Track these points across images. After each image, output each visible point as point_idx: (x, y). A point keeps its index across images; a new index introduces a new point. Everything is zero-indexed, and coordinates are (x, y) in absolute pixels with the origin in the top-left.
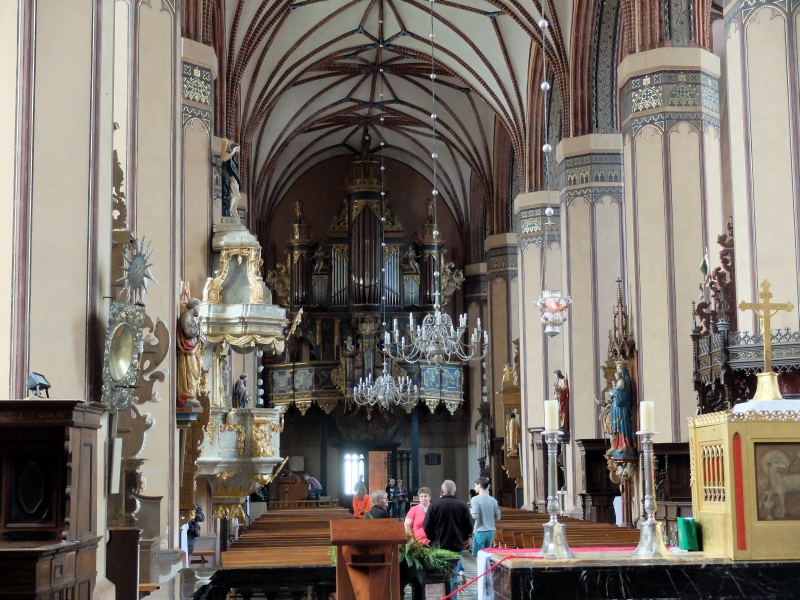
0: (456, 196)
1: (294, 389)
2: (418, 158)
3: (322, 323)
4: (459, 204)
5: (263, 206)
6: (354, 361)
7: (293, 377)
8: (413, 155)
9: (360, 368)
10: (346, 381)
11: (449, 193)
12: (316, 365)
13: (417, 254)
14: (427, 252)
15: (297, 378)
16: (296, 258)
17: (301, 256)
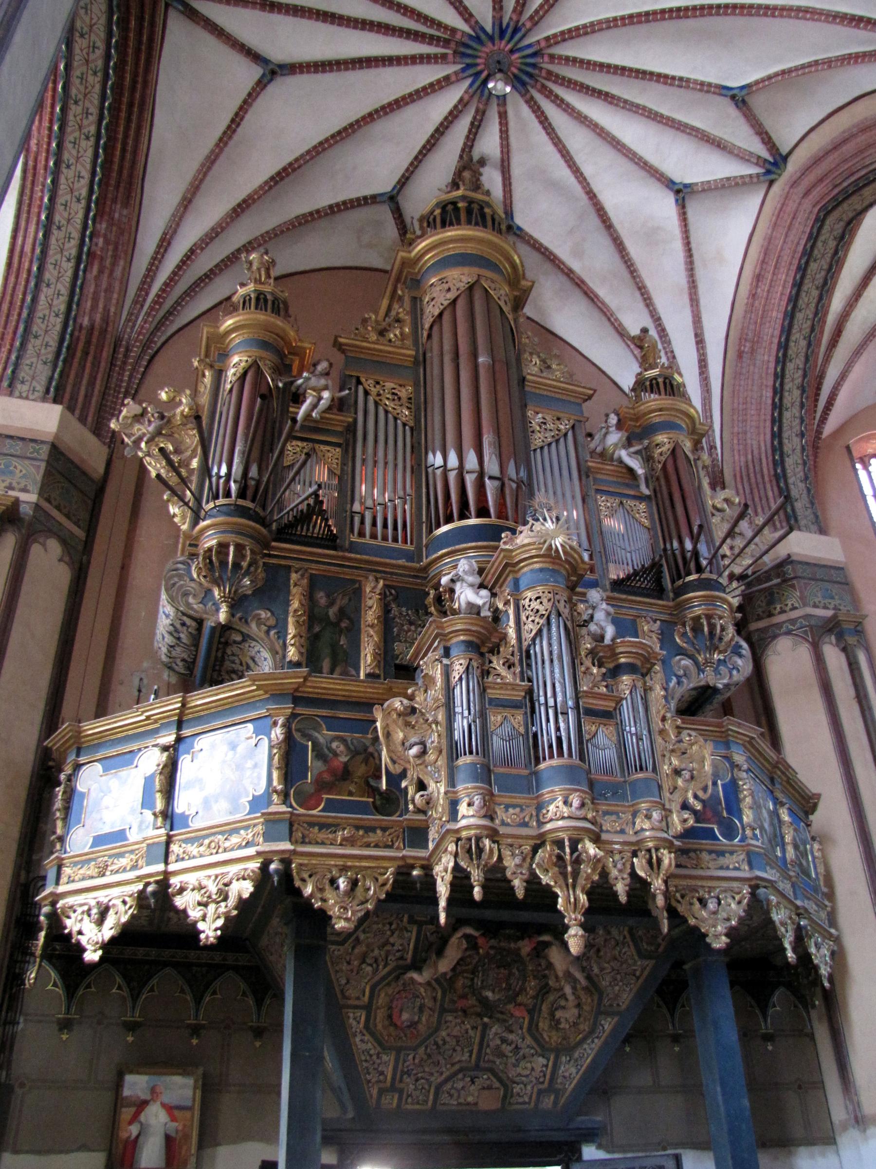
1: (168, 816)
2: (580, 284)
3: (314, 584)
5: (139, 302)
6: (485, 673)
7: (170, 771)
8: (569, 273)
9: (515, 705)
10: (453, 752)
12: (298, 699)
14: (661, 438)
15: (186, 768)
16: (231, 374)
17: (254, 367)
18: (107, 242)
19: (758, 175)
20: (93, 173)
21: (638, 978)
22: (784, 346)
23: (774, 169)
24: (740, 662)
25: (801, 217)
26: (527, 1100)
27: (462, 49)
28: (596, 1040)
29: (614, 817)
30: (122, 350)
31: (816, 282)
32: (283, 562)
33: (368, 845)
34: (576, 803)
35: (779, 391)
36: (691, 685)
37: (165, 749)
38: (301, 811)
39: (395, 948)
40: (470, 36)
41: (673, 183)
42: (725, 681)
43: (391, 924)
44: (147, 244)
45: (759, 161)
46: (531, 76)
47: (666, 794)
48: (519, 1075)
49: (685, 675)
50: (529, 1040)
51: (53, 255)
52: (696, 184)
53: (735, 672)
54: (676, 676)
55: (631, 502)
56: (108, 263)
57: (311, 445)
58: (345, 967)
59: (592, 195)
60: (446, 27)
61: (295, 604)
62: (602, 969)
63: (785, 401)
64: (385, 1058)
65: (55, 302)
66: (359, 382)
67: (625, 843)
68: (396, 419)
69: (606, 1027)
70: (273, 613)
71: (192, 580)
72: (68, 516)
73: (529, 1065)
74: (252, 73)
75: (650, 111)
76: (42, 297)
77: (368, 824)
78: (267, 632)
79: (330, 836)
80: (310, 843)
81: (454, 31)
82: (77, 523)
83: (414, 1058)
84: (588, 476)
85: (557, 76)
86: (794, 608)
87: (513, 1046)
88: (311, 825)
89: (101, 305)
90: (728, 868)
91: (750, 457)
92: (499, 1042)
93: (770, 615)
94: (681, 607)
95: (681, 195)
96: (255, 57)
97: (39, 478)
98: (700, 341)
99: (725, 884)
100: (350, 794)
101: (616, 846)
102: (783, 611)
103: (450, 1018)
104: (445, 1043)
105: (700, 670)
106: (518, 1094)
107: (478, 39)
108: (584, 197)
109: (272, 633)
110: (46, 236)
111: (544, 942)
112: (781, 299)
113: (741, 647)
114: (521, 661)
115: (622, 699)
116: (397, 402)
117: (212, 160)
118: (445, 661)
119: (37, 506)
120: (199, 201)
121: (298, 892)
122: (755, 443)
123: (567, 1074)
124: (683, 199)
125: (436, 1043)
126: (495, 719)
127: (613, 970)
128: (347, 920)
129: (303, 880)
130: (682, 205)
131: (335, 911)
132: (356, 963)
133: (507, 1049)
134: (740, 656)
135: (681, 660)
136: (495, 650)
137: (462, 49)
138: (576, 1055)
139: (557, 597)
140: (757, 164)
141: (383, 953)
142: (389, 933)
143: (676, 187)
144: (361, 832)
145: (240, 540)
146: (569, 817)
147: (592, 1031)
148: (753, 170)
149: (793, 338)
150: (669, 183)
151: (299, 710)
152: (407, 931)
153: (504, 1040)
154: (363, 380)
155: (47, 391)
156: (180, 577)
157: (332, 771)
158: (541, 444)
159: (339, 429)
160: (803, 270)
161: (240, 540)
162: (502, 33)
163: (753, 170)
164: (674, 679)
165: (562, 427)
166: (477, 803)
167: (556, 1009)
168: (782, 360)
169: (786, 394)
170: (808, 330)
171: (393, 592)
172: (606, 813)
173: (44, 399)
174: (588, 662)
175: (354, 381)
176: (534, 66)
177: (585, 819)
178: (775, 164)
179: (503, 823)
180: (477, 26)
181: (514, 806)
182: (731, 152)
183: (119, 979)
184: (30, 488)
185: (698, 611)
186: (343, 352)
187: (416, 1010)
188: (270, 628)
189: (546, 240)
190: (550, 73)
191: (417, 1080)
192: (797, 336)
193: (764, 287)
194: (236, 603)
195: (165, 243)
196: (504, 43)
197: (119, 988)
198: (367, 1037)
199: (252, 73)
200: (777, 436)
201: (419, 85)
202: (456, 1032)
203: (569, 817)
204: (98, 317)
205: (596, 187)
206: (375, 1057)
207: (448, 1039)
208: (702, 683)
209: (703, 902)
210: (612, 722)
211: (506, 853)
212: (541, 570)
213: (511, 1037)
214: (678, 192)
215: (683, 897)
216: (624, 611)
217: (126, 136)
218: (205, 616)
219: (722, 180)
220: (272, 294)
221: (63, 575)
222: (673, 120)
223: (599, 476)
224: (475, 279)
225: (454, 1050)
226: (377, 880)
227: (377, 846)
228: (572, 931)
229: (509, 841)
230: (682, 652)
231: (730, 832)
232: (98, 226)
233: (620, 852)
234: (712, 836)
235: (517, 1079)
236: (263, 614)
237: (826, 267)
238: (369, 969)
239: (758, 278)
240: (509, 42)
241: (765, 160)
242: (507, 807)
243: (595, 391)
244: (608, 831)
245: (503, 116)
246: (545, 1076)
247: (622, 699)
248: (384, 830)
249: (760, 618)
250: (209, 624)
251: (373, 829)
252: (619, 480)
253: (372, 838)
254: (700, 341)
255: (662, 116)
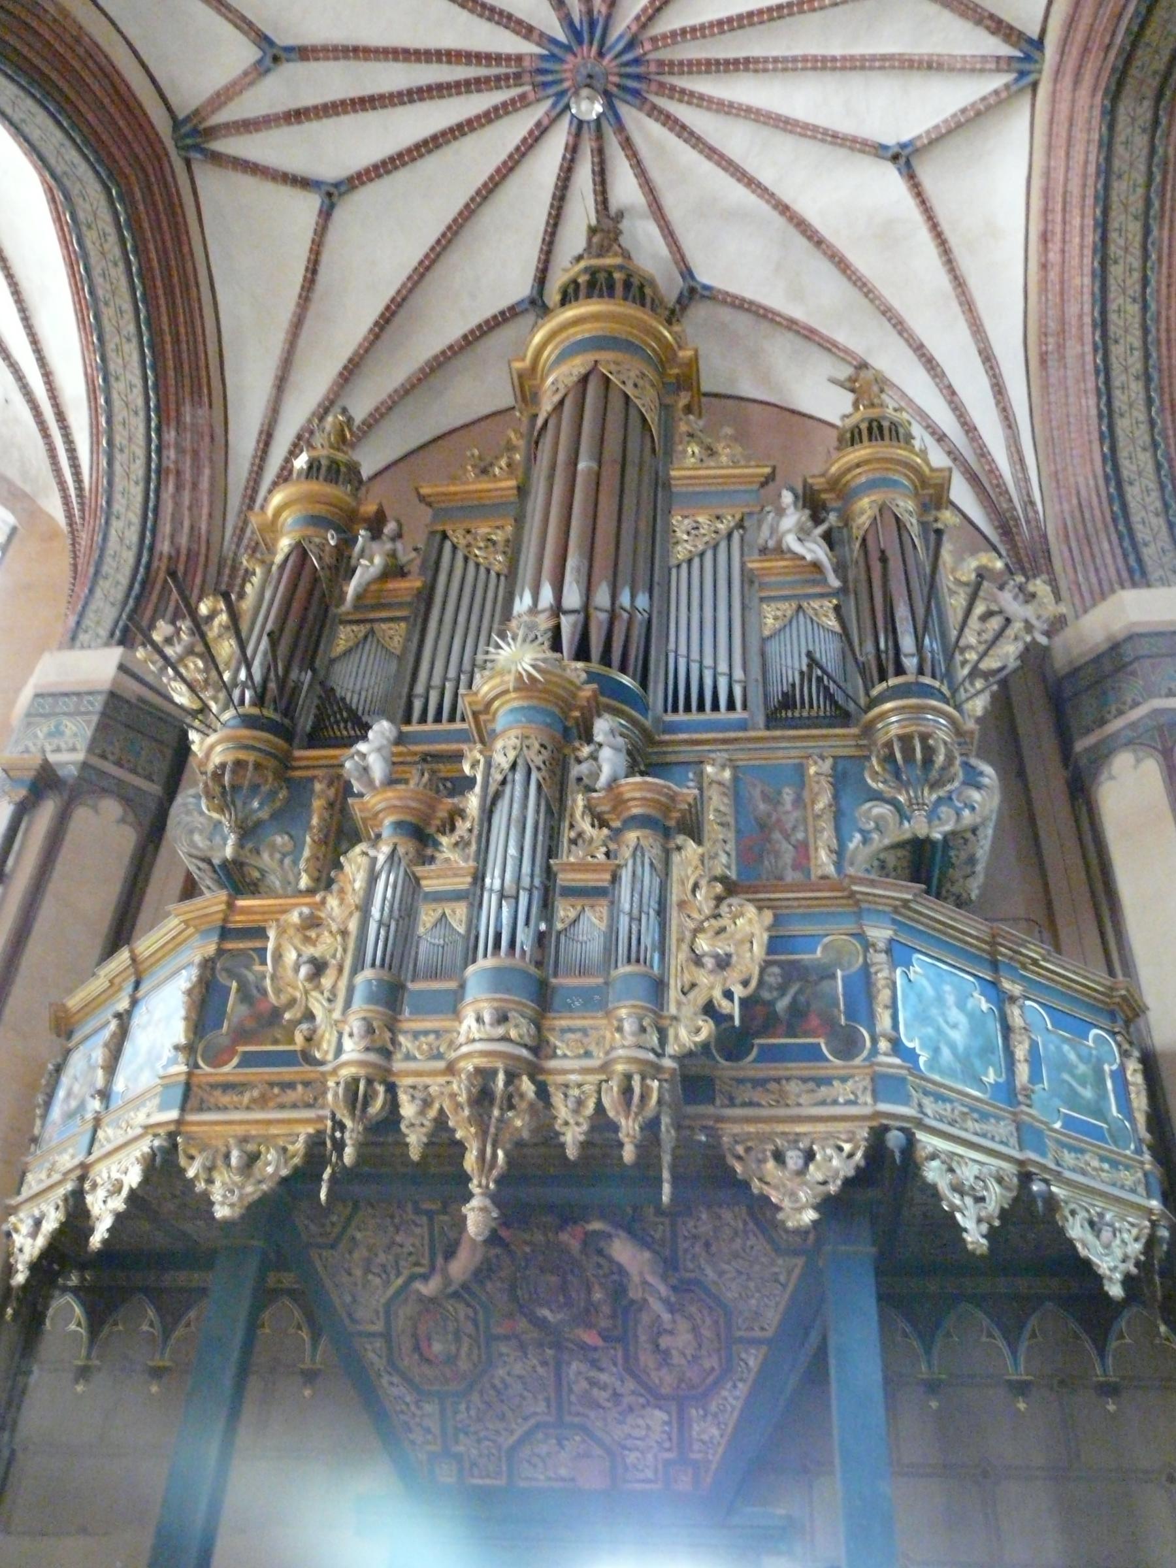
0: (970, 429)
2: (809, 335)
4: (983, 453)
8: (791, 325)
11: (941, 438)
13: (817, 520)
17: (300, 552)
18: (180, 450)
19: (1007, 86)
20: (145, 378)
21: (784, 1286)
22: (1102, 324)
23: (1026, 66)
24: (976, 796)
25: (1080, 121)
26: (650, 1474)
27: (541, 78)
28: (740, 1385)
29: (578, 1035)
30: (227, 571)
31: (1132, 209)
32: (309, 773)
33: (282, 1107)
34: (487, 1018)
35: (1106, 392)
36: (887, 842)
37: (118, 1016)
38: (208, 1069)
39: (405, 1250)
40: (542, 57)
41: (885, 148)
42: (948, 828)
43: (392, 1217)
44: (244, 443)
45: (1000, 64)
46: (638, 77)
47: (673, 994)
48: (629, 1436)
49: (878, 828)
50: (631, 1385)
51: (119, 484)
52: (919, 137)
53: (966, 813)
54: (861, 831)
55: (815, 604)
56: (187, 476)
57: (368, 626)
58: (345, 1279)
59: (784, 209)
60: (508, 58)
61: (315, 821)
62: (721, 1273)
63: (1116, 404)
64: (428, 1408)
65: (127, 533)
66: (445, 536)
67: (585, 1071)
68: (488, 571)
69: (751, 1363)
70: (291, 837)
71: (202, 813)
72: (133, 771)
73: (640, 1422)
74: (308, 205)
75: (815, 59)
76: (113, 532)
77: (287, 1078)
78: (281, 862)
79: (235, 1099)
80: (209, 1109)
81: (519, 58)
82: (149, 778)
83: (468, 1409)
84: (752, 582)
85: (671, 64)
86: (1136, 704)
87: (610, 1391)
88: (214, 1086)
89: (186, 524)
90: (835, 1102)
91: (1075, 501)
92: (584, 1384)
93: (1103, 722)
94: (868, 730)
95: (902, 161)
96: (303, 183)
97: (89, 733)
98: (988, 358)
99: (821, 1128)
100: (276, 1042)
101: (573, 1077)
102: (1121, 713)
103: (504, 1350)
104: (506, 1386)
105: (902, 813)
106: (635, 1466)
107: (553, 57)
108: (775, 215)
109: (287, 861)
110: (110, 463)
111: (594, 1232)
112: (1082, 256)
113: (981, 774)
114: (480, 836)
115: (619, 866)
116: (491, 549)
117: (298, 324)
118: (372, 853)
119: (85, 765)
120: (295, 377)
121: (183, 1171)
122: (1081, 479)
123: (705, 1437)
124: (908, 163)
125: (494, 1387)
126: (427, 916)
127: (740, 1273)
128: (232, 1205)
129: (192, 1158)
130: (910, 176)
131: (216, 1197)
132: (358, 1272)
133: (601, 1396)
134: (978, 787)
135: (870, 809)
136: (449, 826)
137: (541, 78)
138: (713, 1407)
139: (527, 742)
140: (998, 70)
141: (390, 1257)
142: (391, 1229)
143: (890, 153)
144: (276, 1090)
145: (242, 755)
146: (481, 1040)
147: (727, 1370)
148: (998, 81)
149: (1113, 306)
150: (878, 150)
151: (229, 945)
152: (416, 1225)
153: (593, 1383)
154: (450, 533)
155: (112, 634)
156: (188, 813)
157: (258, 1017)
158: (688, 556)
159: (409, 599)
160: (1104, 202)
161: (242, 755)
162: (576, 34)
163: (998, 81)
164: (858, 837)
165: (720, 526)
166: (355, 1031)
167: (659, 1334)
168: (1103, 346)
169: (1117, 393)
170: (1138, 287)
171: (449, 784)
172: (564, 1031)
173: (107, 644)
174: (585, 825)
175: (438, 537)
176: (637, 61)
177: (505, 1039)
178: (1028, 58)
179: (409, 1057)
180: (544, 39)
181: (426, 1033)
182: (951, 69)
183: (151, 1313)
184: (78, 747)
185: (894, 730)
186: (429, 505)
187: (450, 1337)
188: (284, 855)
189: (749, 294)
190: (661, 63)
191: (479, 1441)
192: (1121, 301)
193: (1055, 246)
194: (248, 832)
195: (267, 438)
196: (585, 48)
197: (151, 1325)
198: (395, 1379)
199: (308, 205)
200: (1112, 458)
201: (510, 147)
202: (518, 1369)
203: (481, 1040)
204: (183, 540)
205: (786, 197)
206: (413, 1408)
207: (508, 1379)
208: (907, 836)
209: (779, 1157)
210: (604, 902)
211: (403, 1098)
212: (512, 711)
213: (604, 1377)
214: (895, 158)
215: (748, 1150)
216: (780, 754)
217: (173, 320)
218: (209, 854)
219: (954, 116)
220: (328, 457)
221: (126, 839)
222: (852, 58)
223: (767, 579)
224: (588, 368)
225: (523, 1398)
226: (285, 1150)
227: (294, 1106)
228: (475, 1202)
229: (410, 1081)
230: (878, 797)
231: (848, 1046)
232: (166, 437)
233: (580, 1086)
234: (814, 1054)
235: (629, 1443)
236: (279, 840)
237: (1141, 179)
238: (377, 1281)
239: (1045, 238)
240: (591, 43)
241: (1011, 59)
242: (416, 1035)
243: (774, 468)
244: (565, 1056)
245: (627, 144)
246: (670, 1439)
247: (619, 866)
248: (306, 1084)
249: (1088, 731)
250: (216, 861)
251: (291, 1085)
252: (797, 577)
253: (291, 1096)
254: (988, 358)
255: (834, 59)
